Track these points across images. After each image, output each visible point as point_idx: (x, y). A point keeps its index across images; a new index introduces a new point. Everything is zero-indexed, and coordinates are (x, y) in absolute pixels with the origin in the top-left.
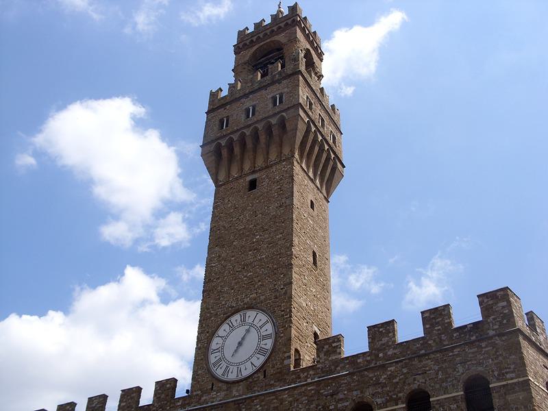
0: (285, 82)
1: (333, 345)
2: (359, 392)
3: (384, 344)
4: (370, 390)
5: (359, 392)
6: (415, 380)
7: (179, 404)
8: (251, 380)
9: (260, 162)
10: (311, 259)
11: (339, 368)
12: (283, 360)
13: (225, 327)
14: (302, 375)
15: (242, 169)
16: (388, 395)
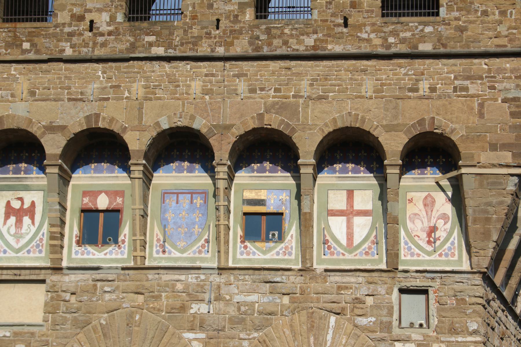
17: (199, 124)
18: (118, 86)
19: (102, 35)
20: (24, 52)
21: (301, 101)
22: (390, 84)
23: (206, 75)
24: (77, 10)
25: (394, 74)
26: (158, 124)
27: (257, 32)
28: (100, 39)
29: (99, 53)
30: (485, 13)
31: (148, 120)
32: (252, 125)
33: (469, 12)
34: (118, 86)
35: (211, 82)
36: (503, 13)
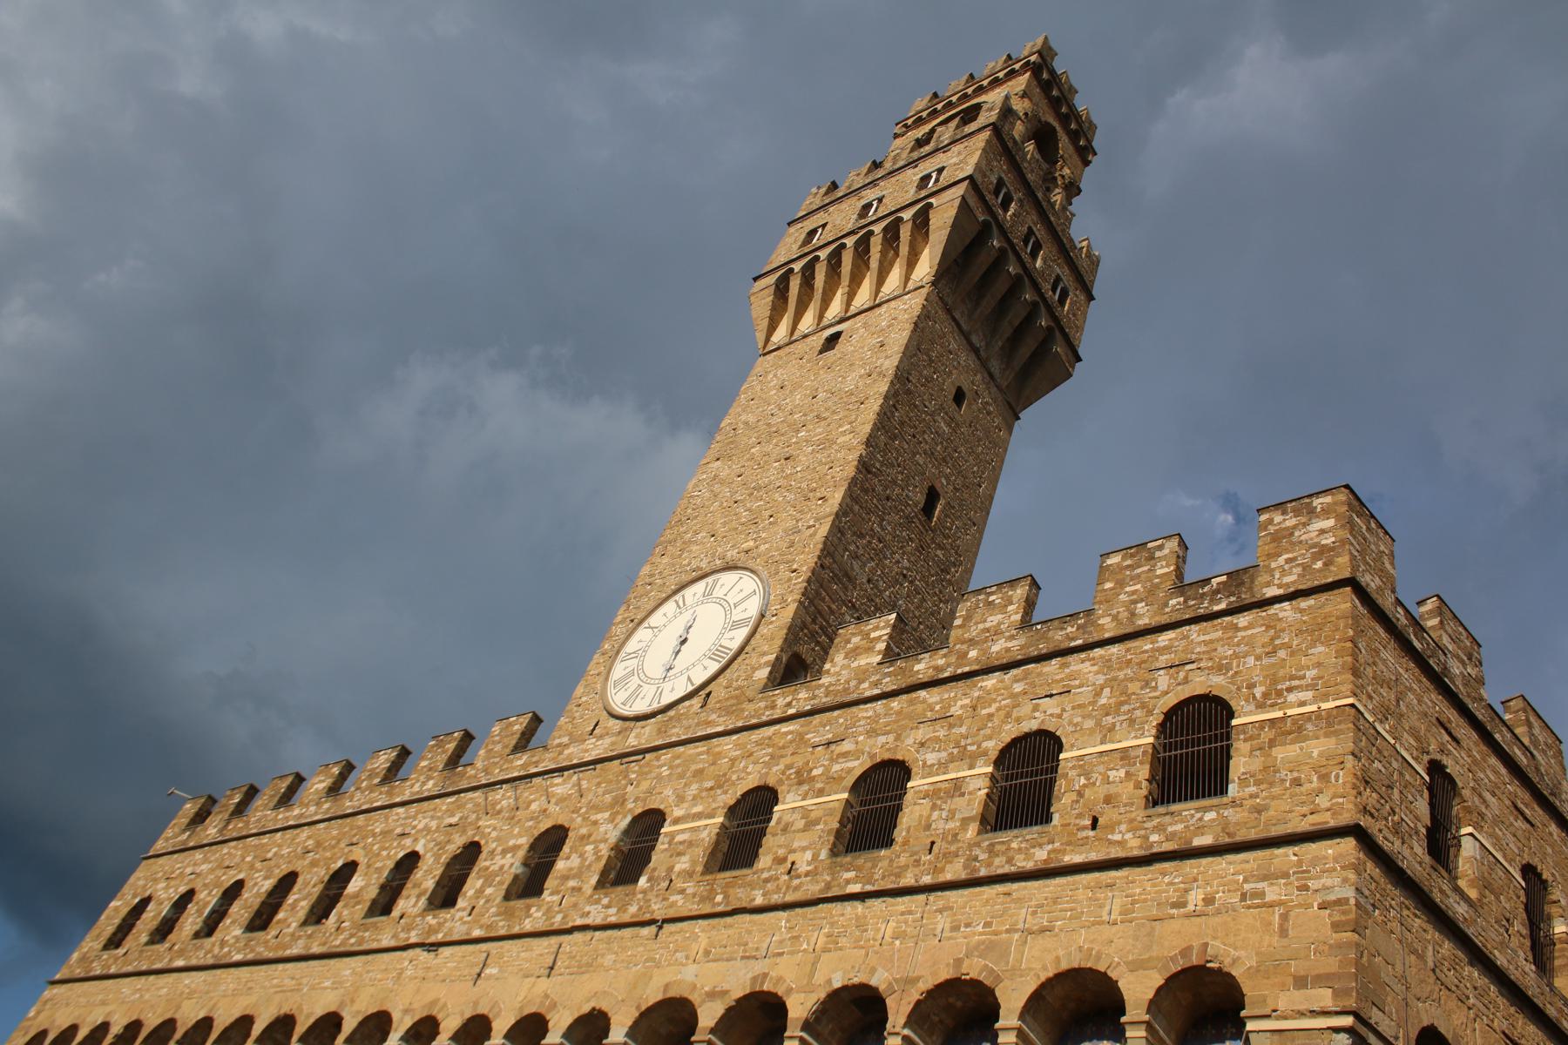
0: (956, 149)
1: (873, 635)
2: (891, 738)
3: (988, 630)
4: (922, 733)
5: (891, 738)
6: (1036, 709)
7: (520, 762)
8: (672, 713)
9: (863, 297)
10: (920, 498)
11: (866, 685)
12: (754, 669)
13: (669, 607)
14: (780, 702)
15: (821, 317)
16: (957, 746)
17: (878, 980)
18: (797, 938)
19: (798, 877)
20: (714, 905)
21: (1016, 936)
22: (1145, 901)
23: (903, 914)
24: (781, 852)
25: (1154, 885)
26: (829, 981)
27: (977, 851)
28: (796, 882)
29: (789, 898)
30: (1297, 782)
31: (819, 978)
32: (945, 974)
33: (1271, 784)
34: (797, 938)
35: (906, 922)
36: (1324, 778)
